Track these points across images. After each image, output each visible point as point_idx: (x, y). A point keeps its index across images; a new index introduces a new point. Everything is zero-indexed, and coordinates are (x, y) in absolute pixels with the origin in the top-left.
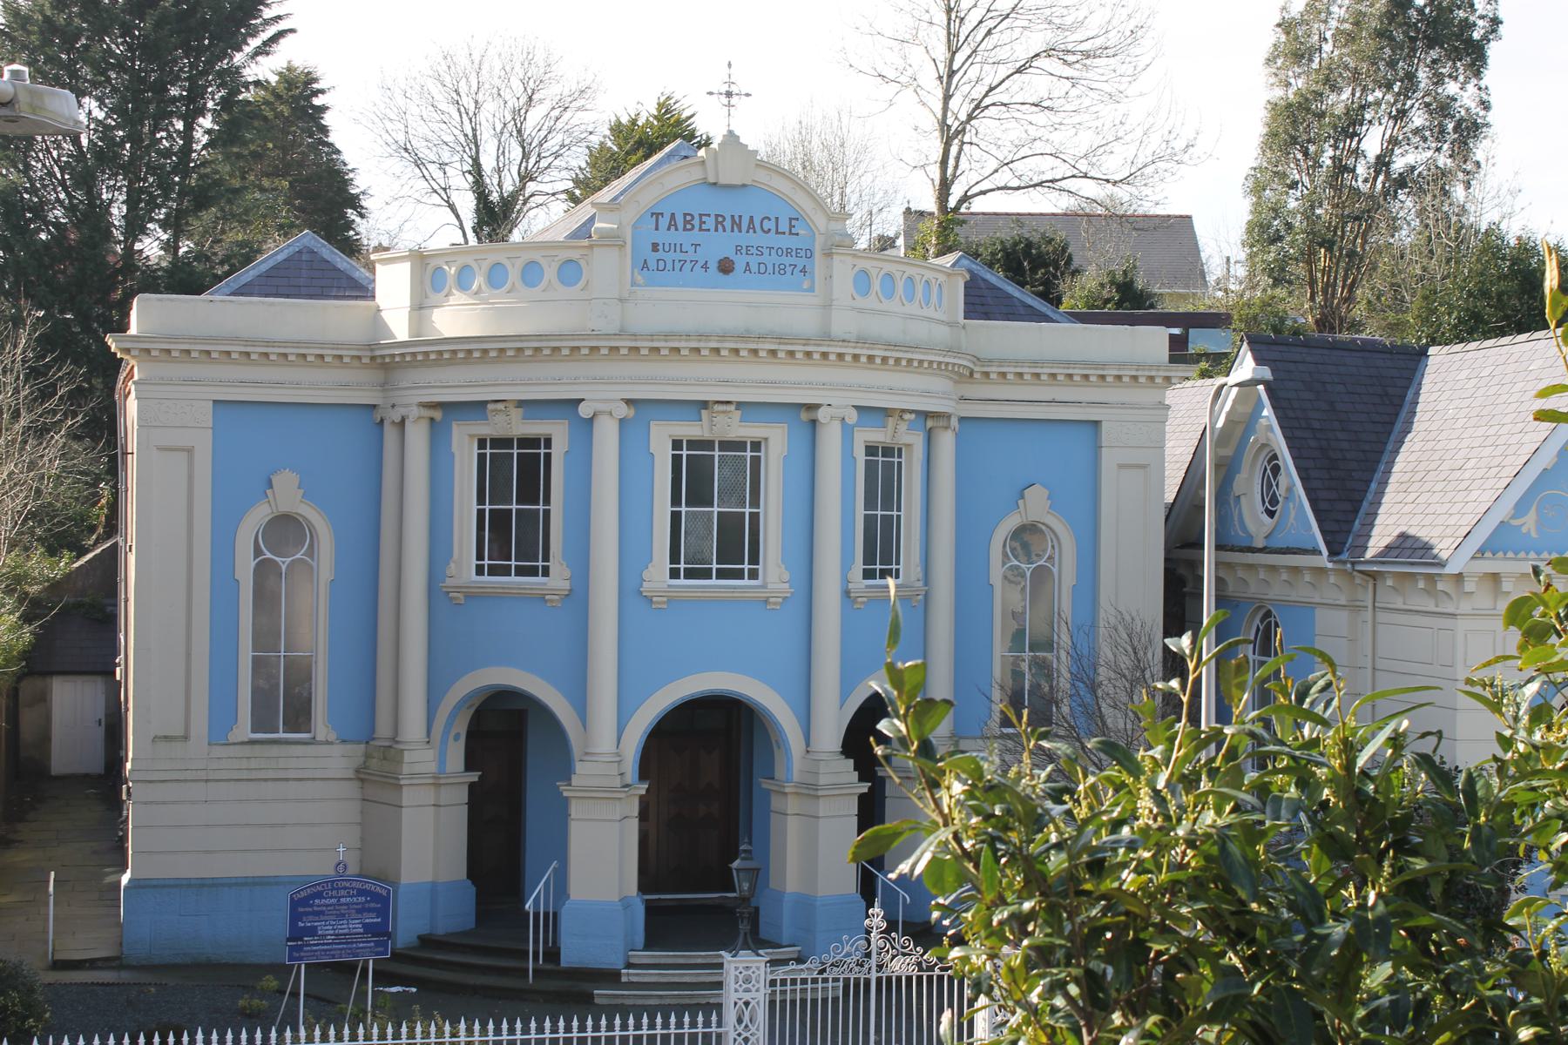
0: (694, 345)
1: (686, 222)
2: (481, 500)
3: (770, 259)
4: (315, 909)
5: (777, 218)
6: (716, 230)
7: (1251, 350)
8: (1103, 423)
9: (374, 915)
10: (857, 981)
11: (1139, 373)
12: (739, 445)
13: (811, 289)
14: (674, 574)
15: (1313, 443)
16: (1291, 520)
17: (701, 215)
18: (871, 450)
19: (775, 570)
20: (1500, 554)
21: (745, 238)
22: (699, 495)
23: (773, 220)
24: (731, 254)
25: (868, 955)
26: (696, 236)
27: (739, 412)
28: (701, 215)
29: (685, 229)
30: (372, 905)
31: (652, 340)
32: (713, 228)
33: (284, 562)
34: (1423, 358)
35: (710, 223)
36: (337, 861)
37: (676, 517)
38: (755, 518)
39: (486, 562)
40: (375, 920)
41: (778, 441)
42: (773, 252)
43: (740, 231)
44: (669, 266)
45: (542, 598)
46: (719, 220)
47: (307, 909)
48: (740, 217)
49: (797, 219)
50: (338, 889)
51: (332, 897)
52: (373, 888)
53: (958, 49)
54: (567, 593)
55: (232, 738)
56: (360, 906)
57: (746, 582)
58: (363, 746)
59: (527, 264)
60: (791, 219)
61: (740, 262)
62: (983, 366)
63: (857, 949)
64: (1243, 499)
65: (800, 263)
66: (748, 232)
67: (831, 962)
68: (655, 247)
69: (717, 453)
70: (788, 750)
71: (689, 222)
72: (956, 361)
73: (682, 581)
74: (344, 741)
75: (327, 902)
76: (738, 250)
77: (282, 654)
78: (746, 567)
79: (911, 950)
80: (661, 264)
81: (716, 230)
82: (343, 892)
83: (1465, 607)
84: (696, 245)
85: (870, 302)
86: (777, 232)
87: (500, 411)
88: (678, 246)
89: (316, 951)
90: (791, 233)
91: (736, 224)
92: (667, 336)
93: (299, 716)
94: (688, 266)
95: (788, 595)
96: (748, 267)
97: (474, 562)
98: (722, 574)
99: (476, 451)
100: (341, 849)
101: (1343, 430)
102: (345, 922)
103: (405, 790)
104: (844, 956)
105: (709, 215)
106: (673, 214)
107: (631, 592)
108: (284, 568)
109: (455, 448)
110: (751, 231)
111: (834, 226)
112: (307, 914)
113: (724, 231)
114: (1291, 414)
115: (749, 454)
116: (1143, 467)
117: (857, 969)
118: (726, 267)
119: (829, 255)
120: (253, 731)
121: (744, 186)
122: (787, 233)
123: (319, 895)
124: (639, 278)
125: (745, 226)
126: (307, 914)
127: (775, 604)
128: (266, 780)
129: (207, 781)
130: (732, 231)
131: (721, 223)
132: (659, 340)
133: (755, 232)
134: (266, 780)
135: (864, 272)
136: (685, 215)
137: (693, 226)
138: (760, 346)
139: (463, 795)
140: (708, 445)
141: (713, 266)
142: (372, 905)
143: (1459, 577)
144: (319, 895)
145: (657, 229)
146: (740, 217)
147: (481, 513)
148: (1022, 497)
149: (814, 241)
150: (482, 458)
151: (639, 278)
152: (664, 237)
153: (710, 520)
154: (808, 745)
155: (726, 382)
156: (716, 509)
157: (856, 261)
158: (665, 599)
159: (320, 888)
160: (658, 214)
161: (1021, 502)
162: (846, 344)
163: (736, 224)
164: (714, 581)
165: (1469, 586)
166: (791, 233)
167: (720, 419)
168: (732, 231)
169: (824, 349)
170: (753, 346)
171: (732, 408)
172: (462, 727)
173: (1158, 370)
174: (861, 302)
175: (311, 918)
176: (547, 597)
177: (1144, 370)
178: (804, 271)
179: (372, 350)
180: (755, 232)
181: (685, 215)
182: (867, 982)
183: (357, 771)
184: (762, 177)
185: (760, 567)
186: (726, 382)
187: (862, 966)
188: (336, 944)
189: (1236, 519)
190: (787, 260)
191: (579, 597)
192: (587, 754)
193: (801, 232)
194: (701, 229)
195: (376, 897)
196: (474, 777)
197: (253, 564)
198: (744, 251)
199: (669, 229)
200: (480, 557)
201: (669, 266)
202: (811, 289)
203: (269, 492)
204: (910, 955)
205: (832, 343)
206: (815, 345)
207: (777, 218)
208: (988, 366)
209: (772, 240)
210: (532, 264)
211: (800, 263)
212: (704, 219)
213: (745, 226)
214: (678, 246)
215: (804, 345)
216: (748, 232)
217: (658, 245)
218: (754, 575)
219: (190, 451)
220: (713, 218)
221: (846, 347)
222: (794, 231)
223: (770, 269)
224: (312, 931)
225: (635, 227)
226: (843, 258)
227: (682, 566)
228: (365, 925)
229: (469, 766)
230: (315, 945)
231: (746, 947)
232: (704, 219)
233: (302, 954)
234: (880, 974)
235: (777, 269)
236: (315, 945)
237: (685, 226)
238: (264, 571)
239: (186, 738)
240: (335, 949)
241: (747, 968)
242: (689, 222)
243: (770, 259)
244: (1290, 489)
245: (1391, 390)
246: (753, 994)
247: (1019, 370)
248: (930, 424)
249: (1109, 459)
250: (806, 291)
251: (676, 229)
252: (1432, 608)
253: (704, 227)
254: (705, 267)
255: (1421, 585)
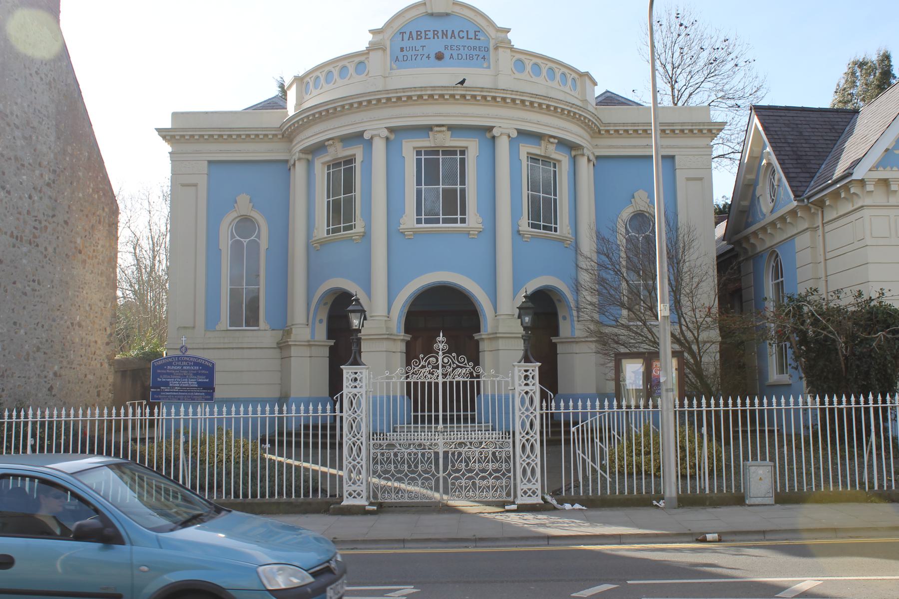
0: (419, 93)
1: (417, 35)
2: (328, 197)
3: (464, 52)
4: (168, 371)
5: (467, 31)
6: (434, 38)
7: (757, 115)
8: (676, 157)
9: (204, 377)
10: (430, 384)
11: (694, 127)
12: (454, 153)
13: (489, 67)
14: (419, 221)
15: (788, 149)
16: (782, 197)
17: (425, 31)
18: (533, 158)
19: (474, 219)
20: (889, 168)
21: (449, 42)
22: (432, 179)
23: (465, 33)
24: (442, 50)
25: (437, 367)
26: (423, 42)
27: (450, 133)
28: (425, 31)
29: (417, 39)
30: (203, 372)
31: (397, 93)
32: (432, 37)
33: (245, 241)
34: (857, 114)
35: (430, 35)
36: (181, 345)
37: (419, 192)
38: (463, 191)
39: (331, 227)
40: (205, 380)
41: (473, 147)
42: (466, 48)
43: (447, 38)
44: (409, 58)
45: (350, 239)
46: (435, 33)
47: (163, 371)
48: (447, 31)
49: (479, 32)
50: (182, 361)
51: (178, 365)
52: (203, 362)
53: (678, 100)
54: (362, 234)
55: (217, 328)
56: (195, 372)
57: (459, 225)
58: (282, 331)
59: (342, 69)
60: (475, 32)
61: (447, 54)
62: (605, 126)
63: (429, 363)
64: (760, 198)
65: (482, 54)
66: (451, 38)
67: (412, 371)
68: (402, 49)
69: (441, 157)
70: (484, 315)
71: (419, 35)
72: (580, 113)
73: (423, 225)
74: (273, 330)
75: (175, 368)
76: (446, 47)
77: (245, 287)
78: (459, 216)
79: (465, 364)
80: (405, 57)
81: (434, 38)
82: (184, 363)
83: (868, 201)
84: (423, 46)
85: (524, 76)
86: (468, 38)
87: (331, 145)
88: (414, 48)
89: (168, 395)
90: (475, 39)
91: (445, 34)
92: (404, 90)
93: (253, 319)
94: (419, 57)
95: (481, 230)
96: (451, 57)
97: (326, 228)
98: (445, 221)
99: (326, 172)
100: (184, 339)
101: (806, 143)
102: (186, 380)
103: (292, 348)
104: (421, 368)
105: (430, 31)
106: (411, 32)
107: (393, 231)
108: (245, 244)
109: (316, 172)
110: (453, 38)
111: (502, 35)
112: (164, 374)
113: (438, 38)
114: (776, 137)
115: (459, 157)
116: (701, 179)
117: (429, 376)
118: (439, 57)
119: (496, 48)
120: (230, 326)
121: (447, 15)
122: (474, 38)
123: (170, 364)
124: (394, 66)
125: (449, 35)
126: (164, 374)
127: (473, 234)
128: (233, 348)
129: (204, 349)
130: (443, 38)
131: (436, 34)
132: (400, 92)
133: (455, 38)
134: (233, 348)
135: (520, 60)
136: (417, 32)
137: (421, 37)
138: (455, 92)
139: (326, 352)
140: (436, 153)
141: (433, 56)
142: (203, 372)
143: (862, 182)
144: (170, 364)
145: (403, 40)
146: (447, 31)
147: (328, 202)
148: (633, 197)
149: (489, 43)
150: (329, 174)
151: (394, 66)
152: (407, 43)
153: (438, 192)
154: (496, 313)
155: (440, 115)
156: (441, 186)
157: (514, 54)
158: (412, 233)
159: (171, 360)
160: (403, 33)
161: (633, 200)
162: (505, 92)
163: (445, 34)
164: (441, 225)
165: (870, 188)
166: (475, 39)
167: (439, 136)
168: (443, 38)
169: (494, 94)
170: (452, 92)
171: (444, 129)
172: (324, 315)
173: (704, 125)
174: (518, 75)
175: (165, 376)
176: (354, 238)
177: (696, 126)
178: (484, 58)
179: (282, 130)
180: (455, 38)
181: (417, 32)
182: (437, 384)
183: (278, 343)
184: (457, 9)
185: (466, 217)
186: (440, 115)
187: (433, 374)
188: (181, 392)
189: (759, 211)
190: (474, 53)
191: (366, 235)
192: (371, 317)
193: (482, 38)
194: (425, 38)
195: (205, 367)
196: (332, 343)
197: (230, 242)
198: (449, 48)
199: (409, 40)
200: (328, 225)
201: (409, 58)
202: (489, 67)
203: (235, 205)
204: (465, 368)
205: (497, 91)
206: (487, 92)
207: (467, 31)
208: (608, 126)
209: (465, 42)
210: (344, 67)
211: (482, 54)
212: (427, 33)
213: (449, 35)
214: (414, 48)
215: (481, 91)
216: (451, 38)
217: (403, 48)
218: (463, 221)
219: (195, 185)
220: (432, 31)
221: (506, 94)
222: (477, 37)
223: (464, 57)
224: (166, 384)
225: (391, 40)
226: (504, 50)
227: (423, 217)
228: (199, 383)
229: (330, 336)
230: (167, 392)
231: (117, 216)
232: (427, 33)
233: (160, 396)
234: (445, 380)
235: (468, 57)
236: (167, 392)
237: (417, 37)
238: (237, 246)
239: (194, 327)
240: (180, 395)
241: (356, 373)
242: (419, 35)
243: (464, 52)
244: (780, 180)
245: (836, 127)
246: (358, 390)
247: (626, 128)
248: (573, 153)
249: (680, 175)
250: (486, 68)
251: (413, 39)
252: (851, 208)
253: (427, 37)
254: (428, 57)
255: (843, 195)
